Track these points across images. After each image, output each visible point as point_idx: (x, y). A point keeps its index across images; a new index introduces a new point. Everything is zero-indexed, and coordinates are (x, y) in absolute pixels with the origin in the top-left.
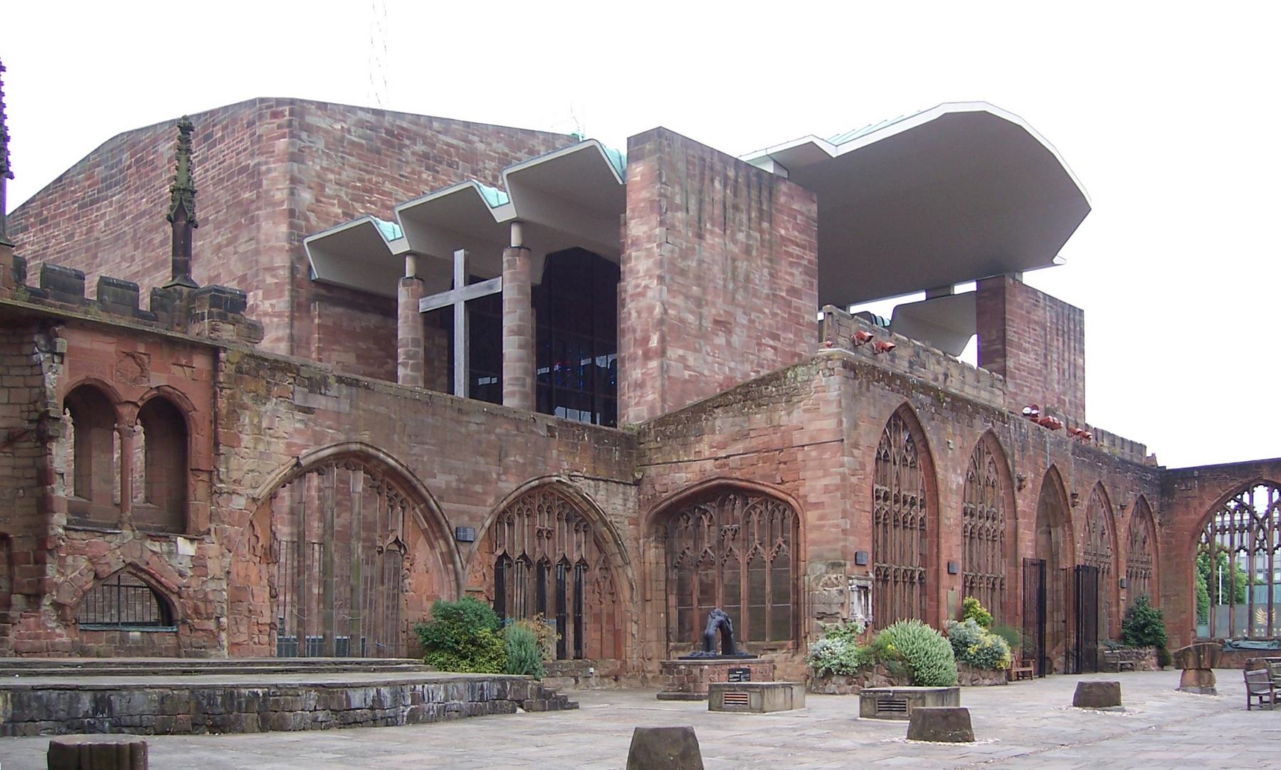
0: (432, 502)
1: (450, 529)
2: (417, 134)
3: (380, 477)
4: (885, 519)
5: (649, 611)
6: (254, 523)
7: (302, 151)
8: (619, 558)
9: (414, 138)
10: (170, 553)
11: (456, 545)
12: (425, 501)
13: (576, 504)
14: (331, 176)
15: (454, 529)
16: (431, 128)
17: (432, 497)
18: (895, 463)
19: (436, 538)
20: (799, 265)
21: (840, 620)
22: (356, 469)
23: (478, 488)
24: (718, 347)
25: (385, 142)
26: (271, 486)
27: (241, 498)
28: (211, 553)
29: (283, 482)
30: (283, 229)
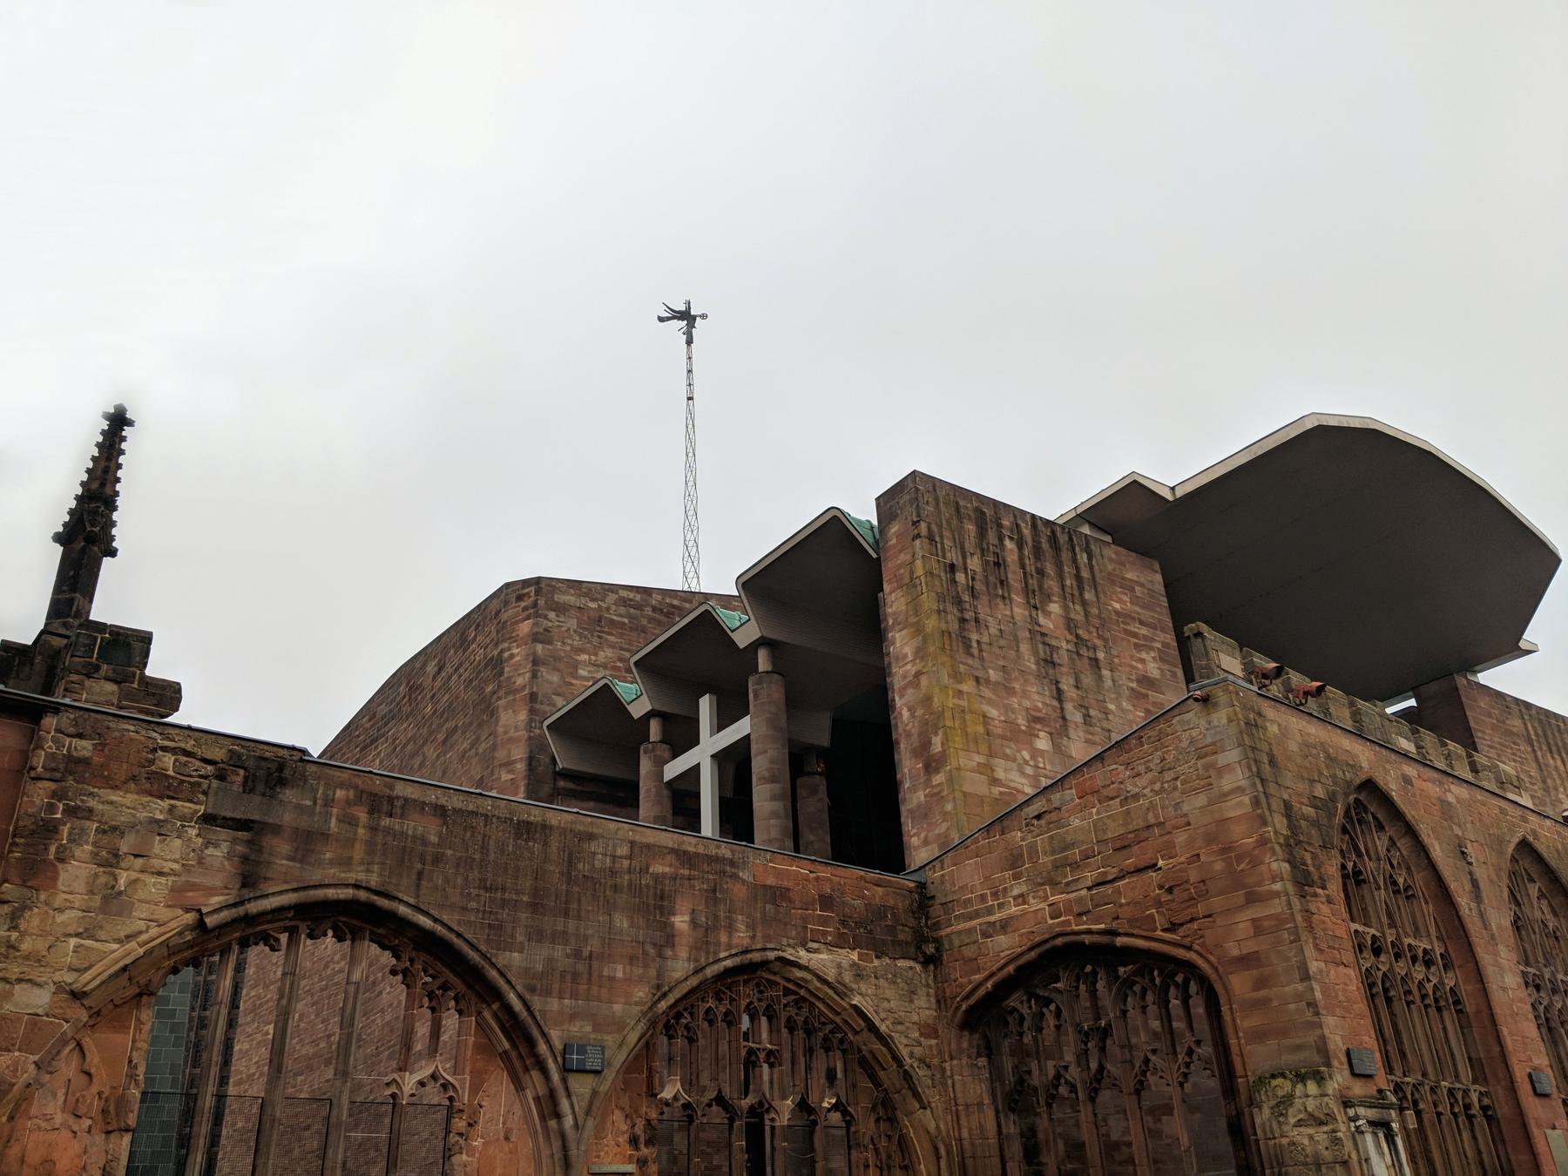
7: (549, 632)
14: (584, 657)
30: (523, 716)
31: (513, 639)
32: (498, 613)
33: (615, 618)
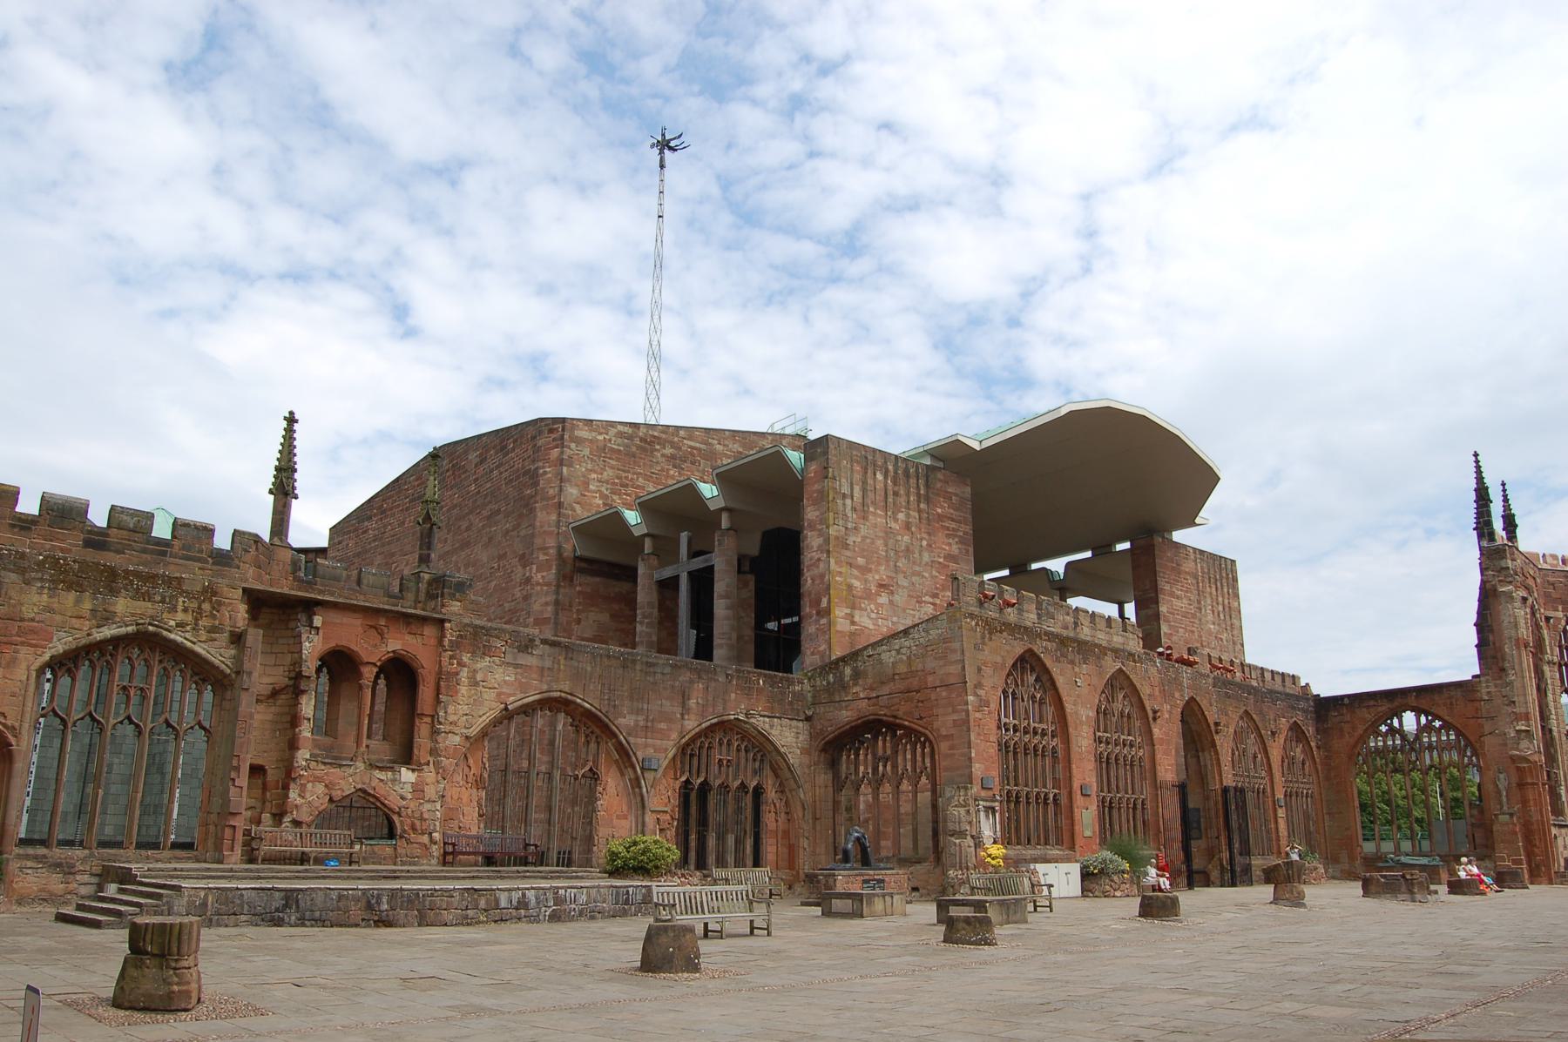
0: (621, 737)
1: (637, 759)
2: (666, 441)
3: (578, 718)
4: (1015, 748)
5: (818, 828)
6: (468, 755)
8: (792, 782)
9: (662, 443)
10: (393, 781)
11: (642, 773)
12: (615, 736)
13: (754, 738)
14: (594, 476)
15: (640, 759)
16: (677, 436)
17: (622, 733)
18: (1023, 701)
19: (626, 767)
20: (956, 536)
21: (969, 837)
22: (559, 711)
23: (663, 726)
24: (881, 605)
25: (638, 447)
26: (482, 726)
27: (455, 736)
28: (428, 780)
29: (494, 722)
31: (547, 460)
32: (534, 438)
33: (614, 446)
